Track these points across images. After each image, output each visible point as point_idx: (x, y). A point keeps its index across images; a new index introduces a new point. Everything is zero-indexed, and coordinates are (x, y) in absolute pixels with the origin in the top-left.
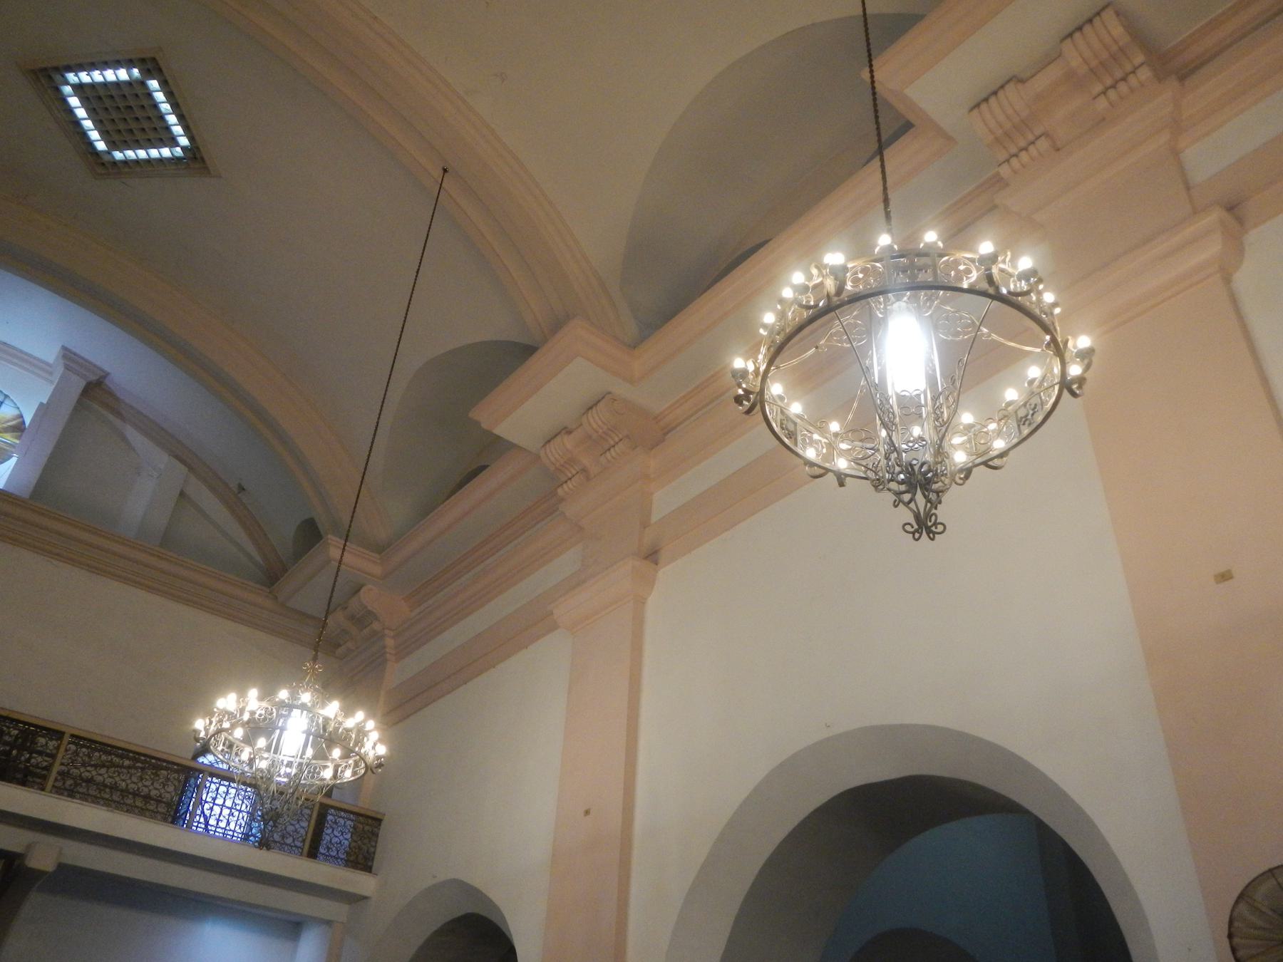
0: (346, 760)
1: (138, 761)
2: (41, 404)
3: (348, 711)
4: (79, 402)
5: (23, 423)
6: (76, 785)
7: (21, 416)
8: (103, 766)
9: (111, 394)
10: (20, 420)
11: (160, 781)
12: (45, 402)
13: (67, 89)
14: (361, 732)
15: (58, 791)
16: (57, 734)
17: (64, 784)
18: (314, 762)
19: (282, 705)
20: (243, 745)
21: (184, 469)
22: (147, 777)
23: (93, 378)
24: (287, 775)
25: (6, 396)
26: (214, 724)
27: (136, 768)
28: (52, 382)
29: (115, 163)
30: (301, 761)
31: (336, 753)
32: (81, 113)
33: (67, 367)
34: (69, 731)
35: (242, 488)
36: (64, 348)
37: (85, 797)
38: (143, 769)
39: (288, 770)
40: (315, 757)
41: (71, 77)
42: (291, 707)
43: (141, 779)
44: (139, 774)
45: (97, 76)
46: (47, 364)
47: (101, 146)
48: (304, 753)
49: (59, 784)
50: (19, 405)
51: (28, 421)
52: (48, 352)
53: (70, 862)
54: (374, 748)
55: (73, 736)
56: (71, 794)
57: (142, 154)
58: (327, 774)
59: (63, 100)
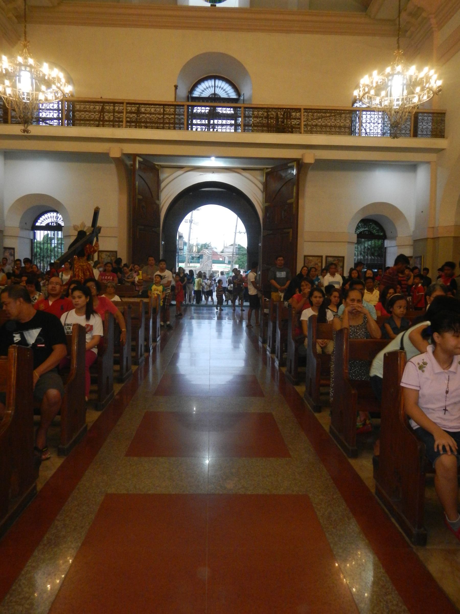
0: (423, 92)
1: (332, 113)
3: (420, 69)
6: (312, 128)
8: (319, 118)
11: (343, 119)
14: (428, 78)
15: (306, 132)
16: (298, 110)
17: (307, 129)
18: (408, 96)
19: (389, 75)
20: (376, 97)
22: (338, 119)
24: (398, 105)
26: (361, 91)
27: (332, 116)
30: (403, 97)
31: (418, 89)
34: (302, 108)
37: (316, 132)
38: (335, 116)
39: (398, 103)
40: (409, 94)
42: (392, 75)
43: (335, 120)
44: (334, 118)
48: (403, 94)
49: (306, 129)
53: (318, 158)
54: (435, 83)
55: (304, 109)
56: (311, 132)
58: (416, 100)
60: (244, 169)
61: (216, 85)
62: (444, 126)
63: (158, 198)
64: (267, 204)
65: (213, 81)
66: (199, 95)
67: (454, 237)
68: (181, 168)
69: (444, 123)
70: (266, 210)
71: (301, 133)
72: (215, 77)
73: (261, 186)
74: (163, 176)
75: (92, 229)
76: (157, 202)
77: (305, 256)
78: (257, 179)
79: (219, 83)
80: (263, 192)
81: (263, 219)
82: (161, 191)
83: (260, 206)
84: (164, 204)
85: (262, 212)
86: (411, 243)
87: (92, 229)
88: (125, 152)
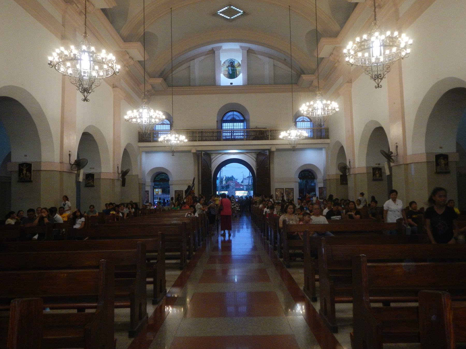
2: (241, 60)
4: (247, 54)
5: (240, 64)
7: (239, 62)
12: (242, 59)
13: (219, 13)
15: (271, 139)
21: (273, 60)
23: (248, 49)
28: (241, 52)
29: (232, 19)
32: (223, 15)
34: (269, 129)
35: (285, 60)
36: (240, 46)
41: (219, 12)
45: (223, 10)
46: (238, 49)
47: (229, 18)
51: (240, 63)
52: (238, 47)
57: (236, 16)
59: (219, 15)
60: (247, 152)
62: (329, 134)
63: (211, 167)
64: (257, 167)
65: (232, 112)
68: (220, 153)
70: (257, 170)
71: (269, 140)
72: (233, 111)
73: (255, 159)
74: (212, 157)
75: (193, 185)
76: (210, 168)
77: (276, 189)
78: (253, 156)
79: (235, 113)
80: (256, 162)
83: (255, 169)
85: (256, 170)
86: (323, 181)
87: (193, 185)
88: (197, 150)
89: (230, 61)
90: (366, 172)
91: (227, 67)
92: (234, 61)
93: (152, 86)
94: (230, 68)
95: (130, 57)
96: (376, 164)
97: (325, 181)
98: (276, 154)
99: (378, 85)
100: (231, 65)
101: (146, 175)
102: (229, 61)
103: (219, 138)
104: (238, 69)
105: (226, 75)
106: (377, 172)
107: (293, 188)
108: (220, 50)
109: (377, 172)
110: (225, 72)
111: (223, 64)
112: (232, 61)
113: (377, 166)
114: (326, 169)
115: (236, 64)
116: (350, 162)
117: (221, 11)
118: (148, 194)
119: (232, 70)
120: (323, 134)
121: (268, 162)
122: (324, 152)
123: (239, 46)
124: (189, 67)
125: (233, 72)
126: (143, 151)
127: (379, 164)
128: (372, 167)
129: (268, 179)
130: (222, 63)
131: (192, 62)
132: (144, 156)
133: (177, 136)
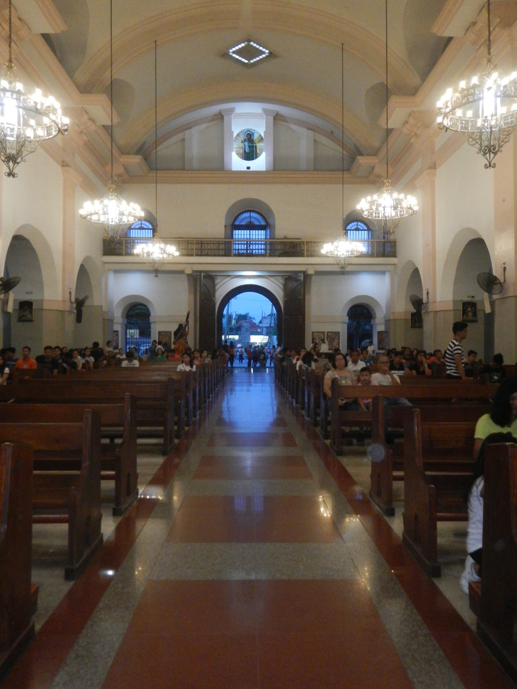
4: (274, 122)
5: (262, 137)
7: (260, 135)
9: (281, 116)
10: (260, 137)
12: (265, 130)
13: (231, 54)
15: (307, 256)
23: (274, 114)
25: (254, 130)
28: (264, 119)
29: (252, 63)
32: (237, 57)
33: (266, 115)
34: (305, 241)
35: (332, 132)
36: (263, 109)
41: (231, 51)
45: (237, 48)
46: (260, 114)
47: (246, 61)
50: (259, 131)
51: (263, 135)
52: (260, 111)
57: (258, 59)
59: (231, 56)
60: (270, 276)
61: (251, 215)
63: (214, 296)
65: (249, 213)
66: (240, 223)
67: (405, 319)
69: (396, 248)
70: (286, 302)
71: (304, 256)
72: (250, 211)
73: (282, 286)
74: (217, 281)
75: (186, 323)
76: (214, 299)
77: (313, 333)
78: (279, 282)
79: (253, 215)
81: (284, 309)
82: (216, 291)
83: (282, 300)
84: (218, 300)
88: (194, 269)
89: (247, 133)
90: (452, 309)
91: (242, 142)
92: (253, 131)
93: (124, 168)
94: (246, 143)
95: (90, 119)
96: (469, 297)
97: (388, 322)
98: (314, 278)
99: (490, 163)
100: (249, 139)
101: (114, 306)
102: (246, 132)
103: (227, 253)
104: (259, 145)
105: (240, 154)
106: (469, 309)
107: (339, 331)
108: (231, 114)
109: (469, 309)
110: (239, 149)
111: (236, 137)
112: (250, 133)
113: (469, 299)
114: (390, 305)
115: (256, 137)
116: (428, 293)
117: (234, 49)
118: (117, 335)
119: (249, 146)
120: (388, 249)
121: (302, 290)
122: (387, 278)
123: (261, 109)
124: (184, 140)
125: (250, 150)
126: (109, 270)
127: (473, 297)
128: (461, 301)
129: (301, 317)
130: (235, 135)
131: (187, 132)
132: (112, 278)
133: (162, 245)
